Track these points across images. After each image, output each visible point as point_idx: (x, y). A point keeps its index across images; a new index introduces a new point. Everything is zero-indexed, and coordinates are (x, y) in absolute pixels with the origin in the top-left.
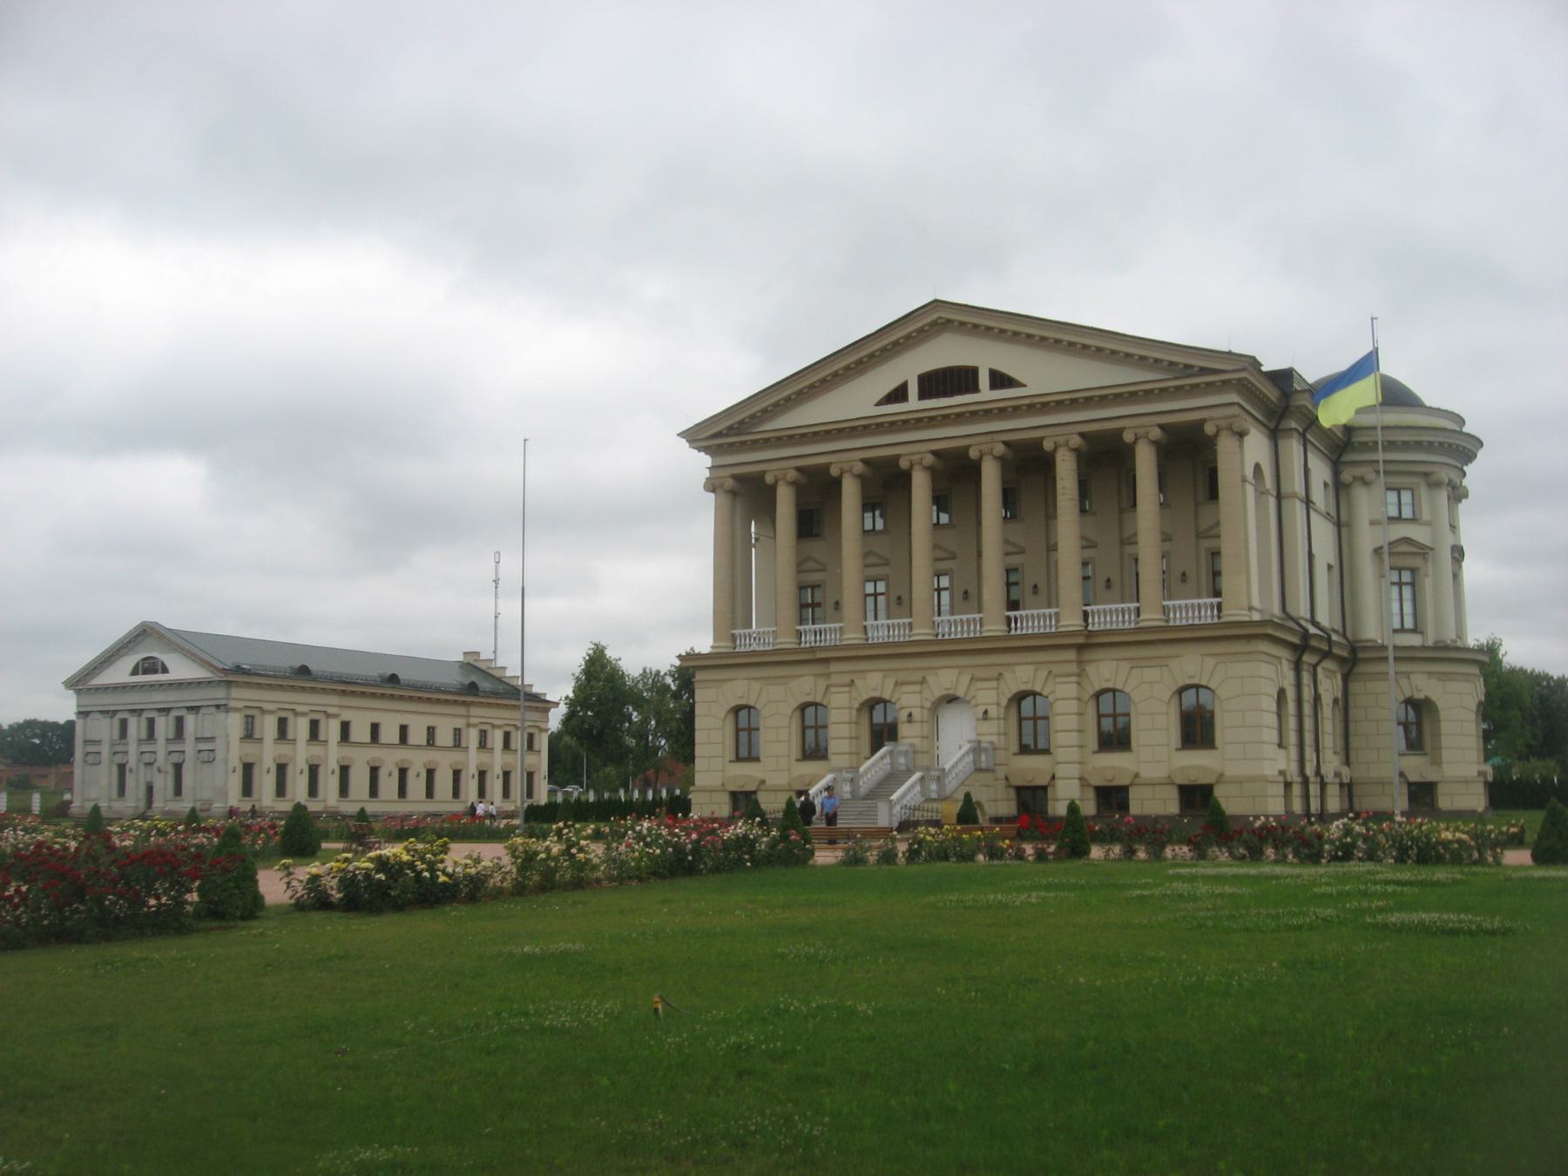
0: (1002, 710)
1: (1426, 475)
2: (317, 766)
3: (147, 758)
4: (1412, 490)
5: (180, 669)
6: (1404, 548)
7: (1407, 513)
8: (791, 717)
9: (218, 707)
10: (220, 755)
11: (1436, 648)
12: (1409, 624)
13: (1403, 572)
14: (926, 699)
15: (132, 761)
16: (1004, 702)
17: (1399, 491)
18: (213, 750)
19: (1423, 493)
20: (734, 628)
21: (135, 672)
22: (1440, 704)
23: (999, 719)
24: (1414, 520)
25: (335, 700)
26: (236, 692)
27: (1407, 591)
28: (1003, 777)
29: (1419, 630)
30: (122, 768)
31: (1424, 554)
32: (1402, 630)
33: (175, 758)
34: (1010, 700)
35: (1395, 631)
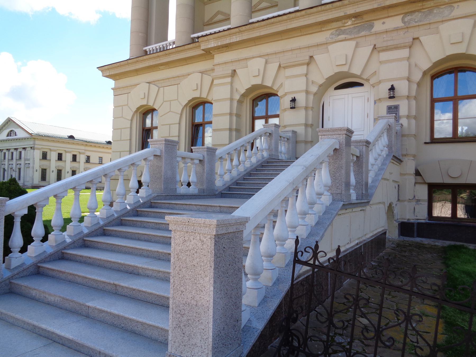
0: (415, 87)
2: (45, 170)
3: (10, 166)
5: (21, 134)
8: (181, 115)
9: (31, 148)
10: (31, 165)
14: (313, 82)
15: (6, 169)
16: (417, 76)
18: (29, 164)
20: (147, 45)
21: (8, 136)
23: (408, 97)
25: (83, 147)
26: (37, 142)
28: (413, 171)
30: (4, 169)
33: (18, 166)
34: (425, 73)
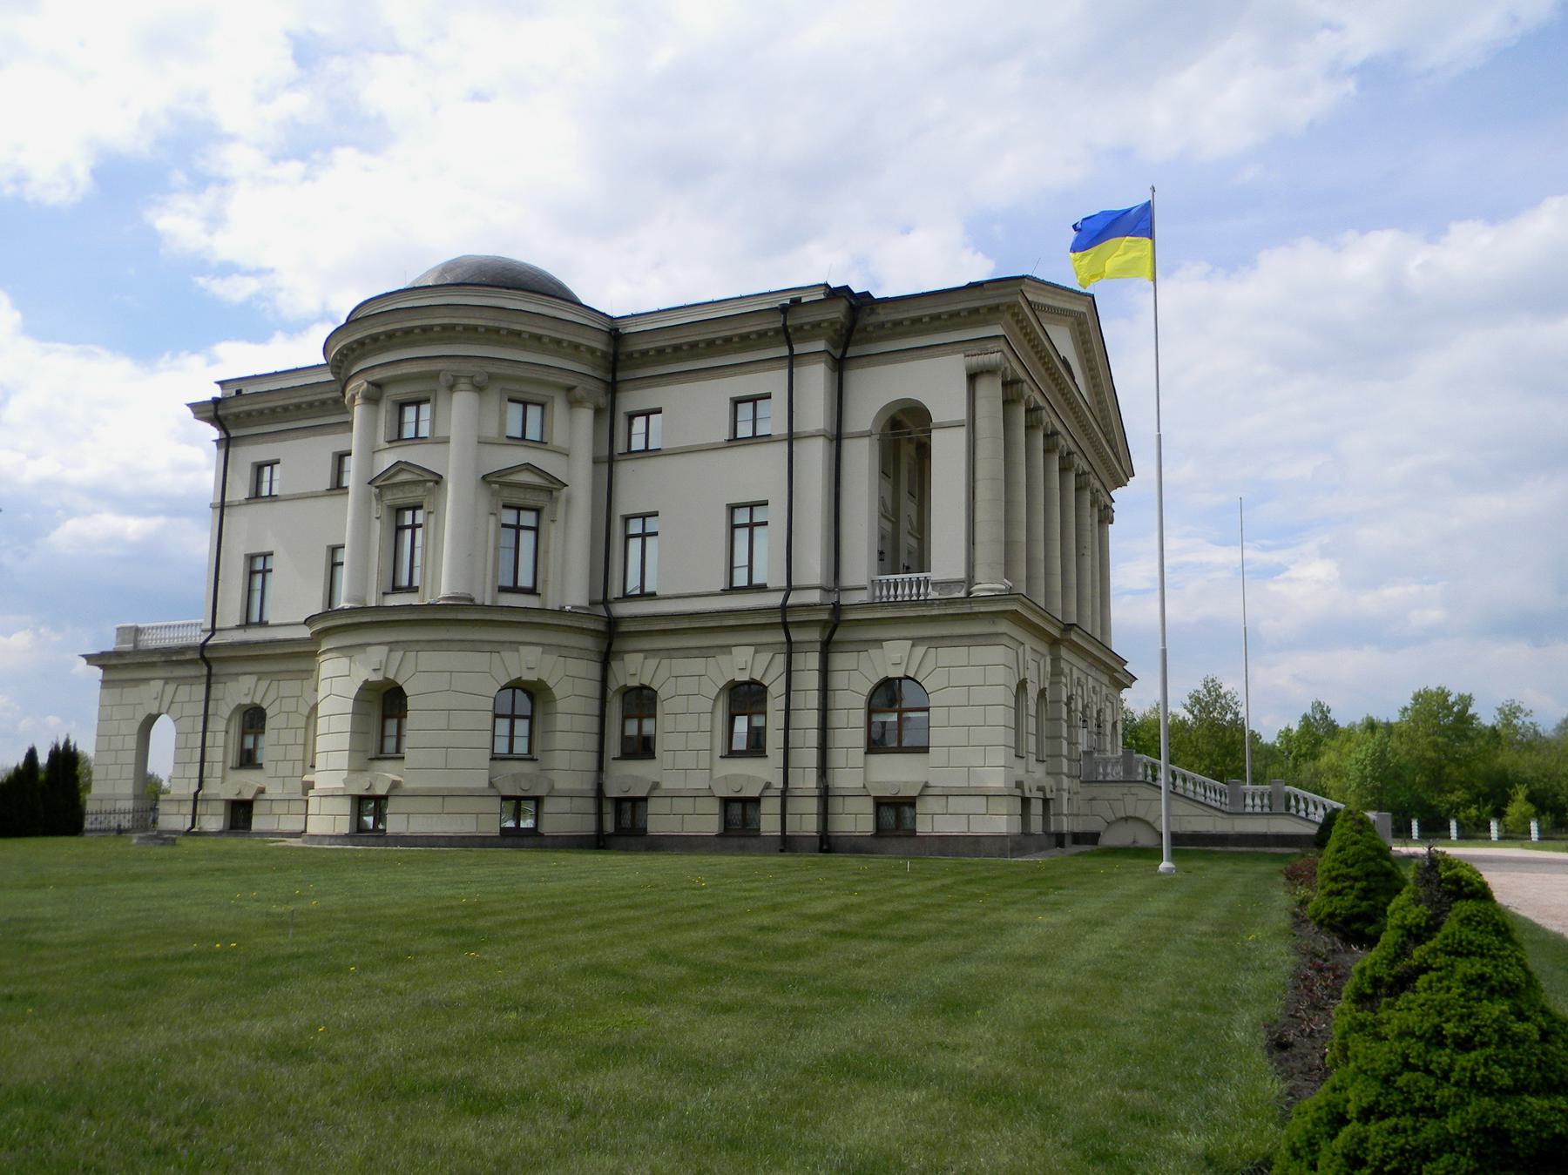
1: (570, 389)
4: (542, 405)
6: (526, 478)
7: (533, 433)
11: (561, 612)
12: (525, 580)
13: (521, 512)
17: (525, 404)
19: (559, 408)
22: (558, 692)
24: (541, 443)
27: (527, 539)
29: (539, 590)
31: (550, 491)
32: (515, 589)
35: (503, 590)
